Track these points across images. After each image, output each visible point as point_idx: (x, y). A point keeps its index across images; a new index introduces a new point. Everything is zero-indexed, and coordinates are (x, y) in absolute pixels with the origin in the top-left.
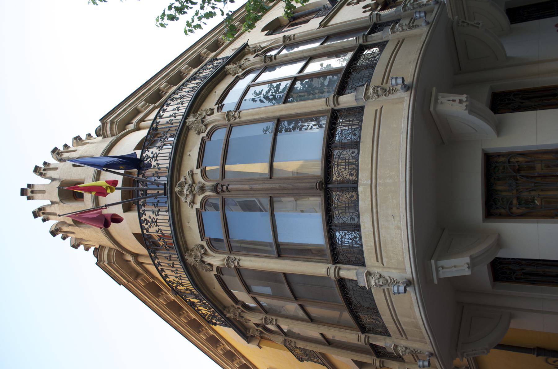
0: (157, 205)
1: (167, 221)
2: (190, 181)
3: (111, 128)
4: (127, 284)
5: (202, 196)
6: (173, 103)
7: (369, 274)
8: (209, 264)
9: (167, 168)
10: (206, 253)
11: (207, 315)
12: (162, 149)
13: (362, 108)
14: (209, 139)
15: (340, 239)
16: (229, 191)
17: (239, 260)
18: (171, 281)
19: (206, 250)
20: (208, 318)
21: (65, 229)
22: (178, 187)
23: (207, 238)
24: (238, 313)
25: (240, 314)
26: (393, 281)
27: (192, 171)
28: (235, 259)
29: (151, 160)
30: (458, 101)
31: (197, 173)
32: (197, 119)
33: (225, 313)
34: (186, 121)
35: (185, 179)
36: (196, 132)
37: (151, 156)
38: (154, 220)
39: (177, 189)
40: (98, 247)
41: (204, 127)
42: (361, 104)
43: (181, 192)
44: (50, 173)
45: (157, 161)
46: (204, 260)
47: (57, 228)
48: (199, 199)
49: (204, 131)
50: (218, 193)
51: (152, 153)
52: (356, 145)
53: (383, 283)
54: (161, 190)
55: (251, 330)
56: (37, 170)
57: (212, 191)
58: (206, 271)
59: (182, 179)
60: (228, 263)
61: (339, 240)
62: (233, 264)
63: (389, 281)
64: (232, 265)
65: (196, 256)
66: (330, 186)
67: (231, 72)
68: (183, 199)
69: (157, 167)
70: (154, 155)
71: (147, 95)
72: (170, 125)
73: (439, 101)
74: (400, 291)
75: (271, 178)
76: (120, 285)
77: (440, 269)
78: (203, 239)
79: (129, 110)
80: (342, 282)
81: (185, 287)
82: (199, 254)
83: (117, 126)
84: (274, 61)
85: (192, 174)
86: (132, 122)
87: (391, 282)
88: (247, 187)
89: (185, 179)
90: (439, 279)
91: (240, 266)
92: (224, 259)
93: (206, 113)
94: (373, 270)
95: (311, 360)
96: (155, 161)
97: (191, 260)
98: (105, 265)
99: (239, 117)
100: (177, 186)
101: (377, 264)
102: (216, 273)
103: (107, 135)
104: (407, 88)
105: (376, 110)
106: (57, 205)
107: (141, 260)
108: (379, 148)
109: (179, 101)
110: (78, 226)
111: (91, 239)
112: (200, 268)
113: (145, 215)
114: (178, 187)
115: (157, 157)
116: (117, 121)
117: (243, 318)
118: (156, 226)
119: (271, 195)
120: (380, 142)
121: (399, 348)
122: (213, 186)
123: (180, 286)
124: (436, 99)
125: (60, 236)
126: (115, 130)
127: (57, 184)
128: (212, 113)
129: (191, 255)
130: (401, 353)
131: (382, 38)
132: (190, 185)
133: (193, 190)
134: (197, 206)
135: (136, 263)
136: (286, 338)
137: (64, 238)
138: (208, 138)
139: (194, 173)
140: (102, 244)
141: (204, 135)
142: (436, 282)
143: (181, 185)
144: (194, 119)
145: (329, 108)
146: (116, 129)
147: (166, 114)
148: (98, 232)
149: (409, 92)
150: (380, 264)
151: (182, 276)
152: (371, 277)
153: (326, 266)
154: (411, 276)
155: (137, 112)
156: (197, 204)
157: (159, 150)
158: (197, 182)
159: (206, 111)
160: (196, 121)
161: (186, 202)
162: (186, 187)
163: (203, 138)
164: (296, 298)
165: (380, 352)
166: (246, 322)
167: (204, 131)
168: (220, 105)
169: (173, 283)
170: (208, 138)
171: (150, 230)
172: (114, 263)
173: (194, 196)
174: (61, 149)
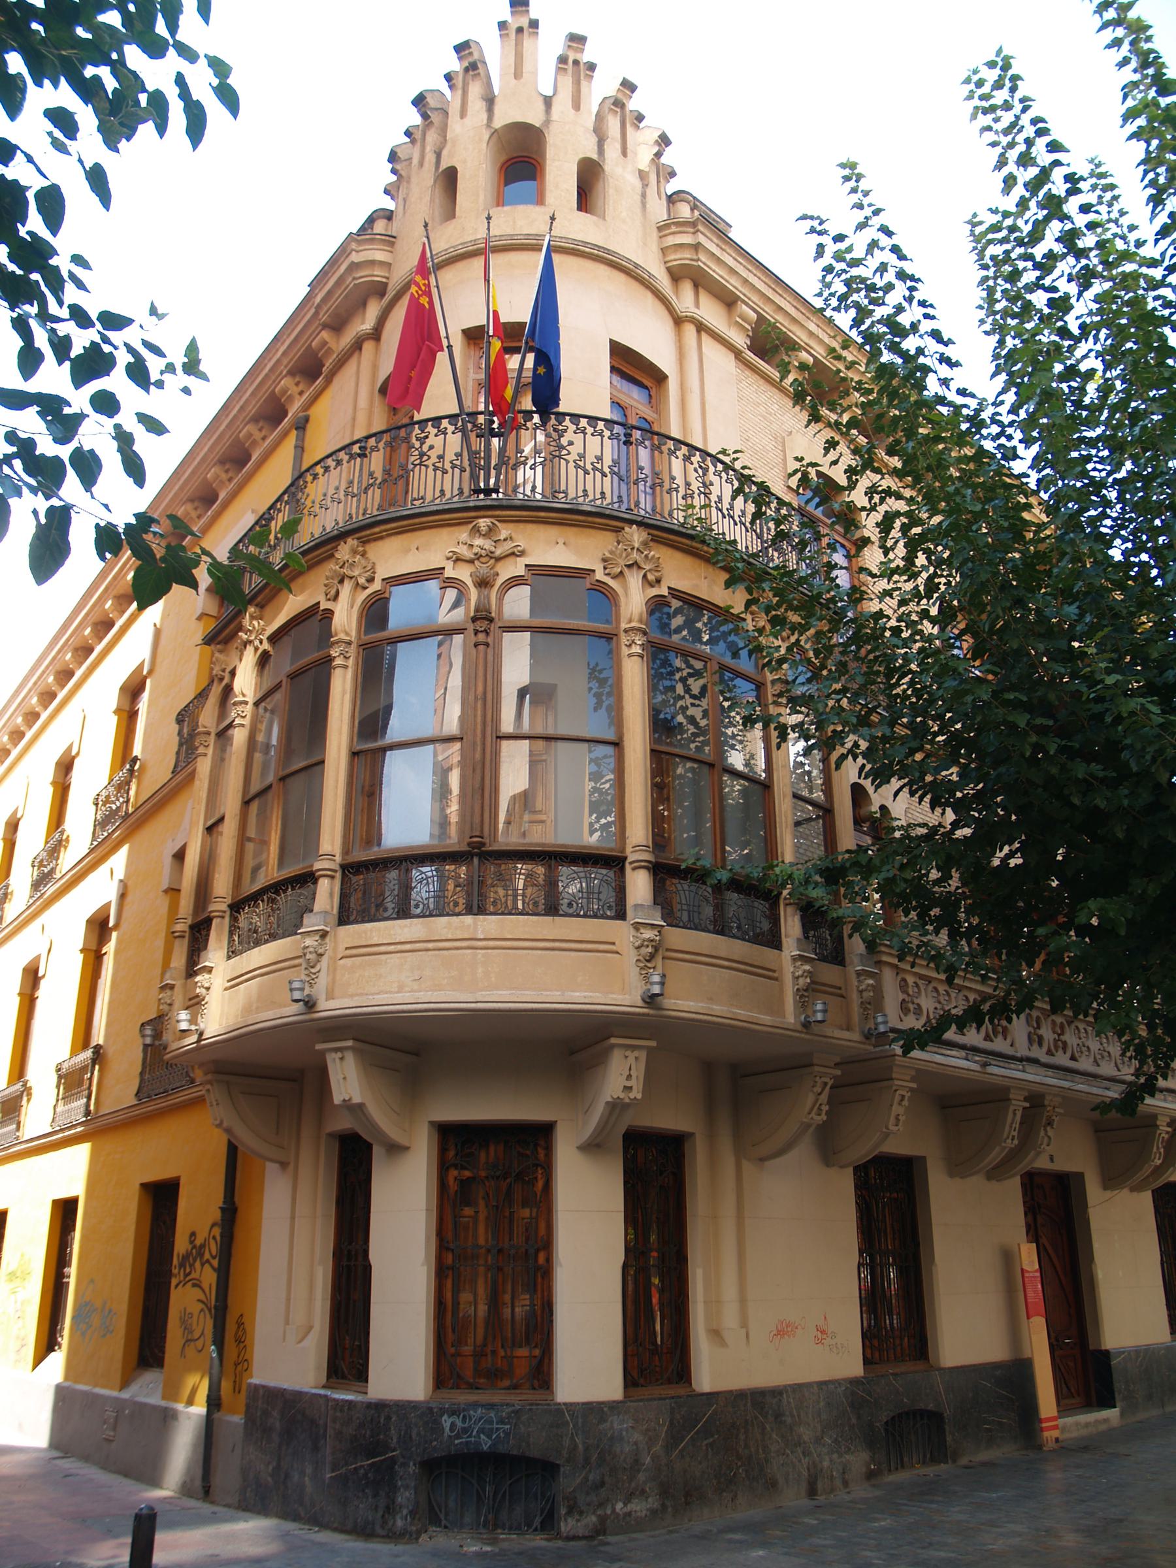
1: (422, 494)
2: (498, 552)
3: (681, 246)
7: (324, 935)
8: (337, 593)
12: (577, 467)
13: (621, 915)
14: (589, 586)
16: (476, 645)
17: (346, 667)
19: (365, 588)
21: (432, 137)
25: (251, 642)
27: (522, 553)
30: (628, 1084)
36: (608, 555)
37: (564, 441)
39: (483, 523)
42: (630, 912)
46: (346, 582)
48: (464, 573)
50: (474, 619)
51: (571, 443)
52: (552, 909)
56: (576, 40)
59: (504, 531)
60: (337, 642)
63: (313, 970)
65: (352, 565)
66: (476, 860)
68: (463, 534)
70: (564, 448)
73: (628, 1053)
75: (498, 737)
77: (339, 1055)
79: (733, 284)
80: (308, 879)
82: (356, 573)
83: (687, 262)
92: (347, 634)
93: (650, 570)
95: (181, 745)
97: (344, 551)
99: (630, 656)
101: (342, 947)
103: (665, 236)
104: (651, 1000)
105: (614, 944)
106: (485, 122)
107: (368, 347)
108: (539, 952)
110: (435, 182)
113: (436, 435)
116: (698, 260)
120: (552, 953)
121: (207, 976)
124: (633, 1048)
125: (415, 119)
127: (535, 117)
129: (354, 552)
130: (198, 978)
133: (483, 560)
134: (449, 572)
136: (213, 736)
141: (599, 575)
142: (318, 1047)
143: (490, 532)
144: (636, 545)
145: (629, 850)
149: (640, 1003)
150: (341, 952)
152: (317, 938)
157: (574, 461)
158: (500, 567)
159: (657, 568)
160: (633, 549)
162: (487, 544)
164: (283, 779)
165: (199, 932)
172: (354, 279)
173: (471, 562)
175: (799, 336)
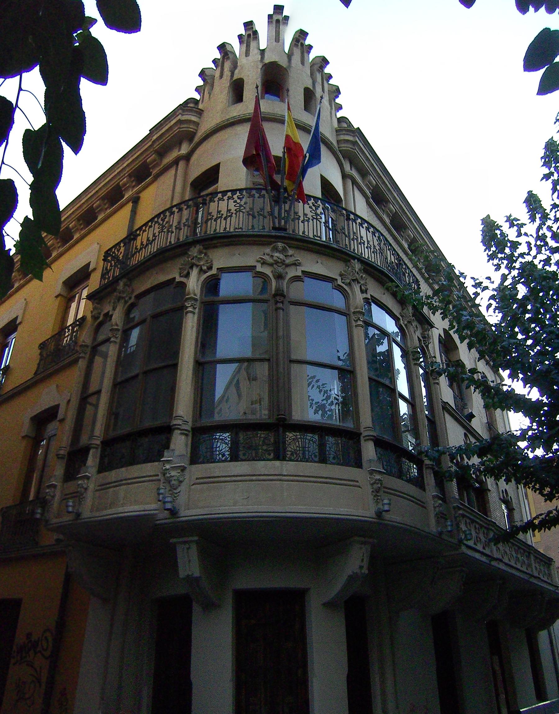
0: (261, 215)
1: (241, 226)
2: (288, 261)
3: (347, 141)
4: (150, 139)
5: (271, 275)
6: (375, 239)
9: (304, 232)
10: (202, 271)
11: (118, 253)
15: (221, 437)
17: (194, 313)
18: (165, 218)
19: (205, 272)
20: (114, 252)
22: (282, 247)
23: (220, 275)
24: (123, 296)
26: (176, 495)
27: (299, 264)
28: (195, 308)
29: (313, 212)
31: (297, 271)
32: (357, 273)
33: (125, 280)
34: (356, 260)
35: (291, 256)
38: (242, 208)
39: (280, 245)
40: (201, 106)
41: (348, 281)
43: (275, 249)
44: (297, 53)
45: (312, 220)
46: (194, 268)
47: (228, 55)
48: (267, 271)
49: (343, 281)
50: (275, 296)
53: (173, 484)
54: (280, 223)
55: (99, 305)
57: (277, 289)
58: (180, 269)
59: (290, 252)
61: (220, 436)
62: (190, 305)
63: (175, 491)
64: (189, 304)
65: (200, 259)
67: (404, 311)
68: (268, 250)
69: (305, 219)
71: (382, 187)
72: (352, 237)
74: (167, 504)
76: (150, 131)
77: (187, 546)
78: (219, 270)
79: (367, 165)
81: (159, 235)
82: (202, 263)
83: (350, 149)
84: (412, 362)
85: (296, 264)
86: (353, 169)
87: (174, 492)
88: (281, 334)
89: (291, 256)
90: (175, 545)
91: (187, 313)
92: (195, 295)
93: (363, 284)
94: (187, 472)
96: (312, 216)
97: (194, 251)
98: (178, 116)
99: (356, 326)
100: (283, 245)
101: (193, 478)
102: (177, 280)
103: (340, 134)
107: (182, 164)
109: (377, 248)
111: (212, 100)
112: (184, 261)
114: (282, 247)
115: (317, 219)
117: (116, 301)
118: (235, 210)
119: (271, 360)
122: (283, 291)
123: (159, 228)
125: (218, 56)
126: (345, 147)
127: (283, 62)
128: (362, 292)
129: (200, 252)
131: (428, 485)
132: (284, 261)
133: (280, 265)
134: (259, 268)
135: (178, 158)
137: (214, 61)
138: (335, 286)
139: (298, 267)
140: (205, 114)
141: (339, 282)
142: (173, 540)
143: (284, 250)
144: (357, 270)
146: (346, 147)
147: (363, 232)
148: (222, 113)
150: (194, 480)
151: (172, 234)
152: (179, 471)
153: (189, 418)
154: (182, 515)
155: (364, 174)
156: (261, 267)
158: (287, 270)
159: (365, 285)
161: (264, 254)
162: (282, 256)
163: (336, 280)
166: (110, 302)
167: (343, 281)
168: (370, 301)
169: (163, 220)
170: (335, 286)
171: (231, 201)
172: (180, 128)
173: (271, 265)
174: (327, 70)
175: (390, 197)
